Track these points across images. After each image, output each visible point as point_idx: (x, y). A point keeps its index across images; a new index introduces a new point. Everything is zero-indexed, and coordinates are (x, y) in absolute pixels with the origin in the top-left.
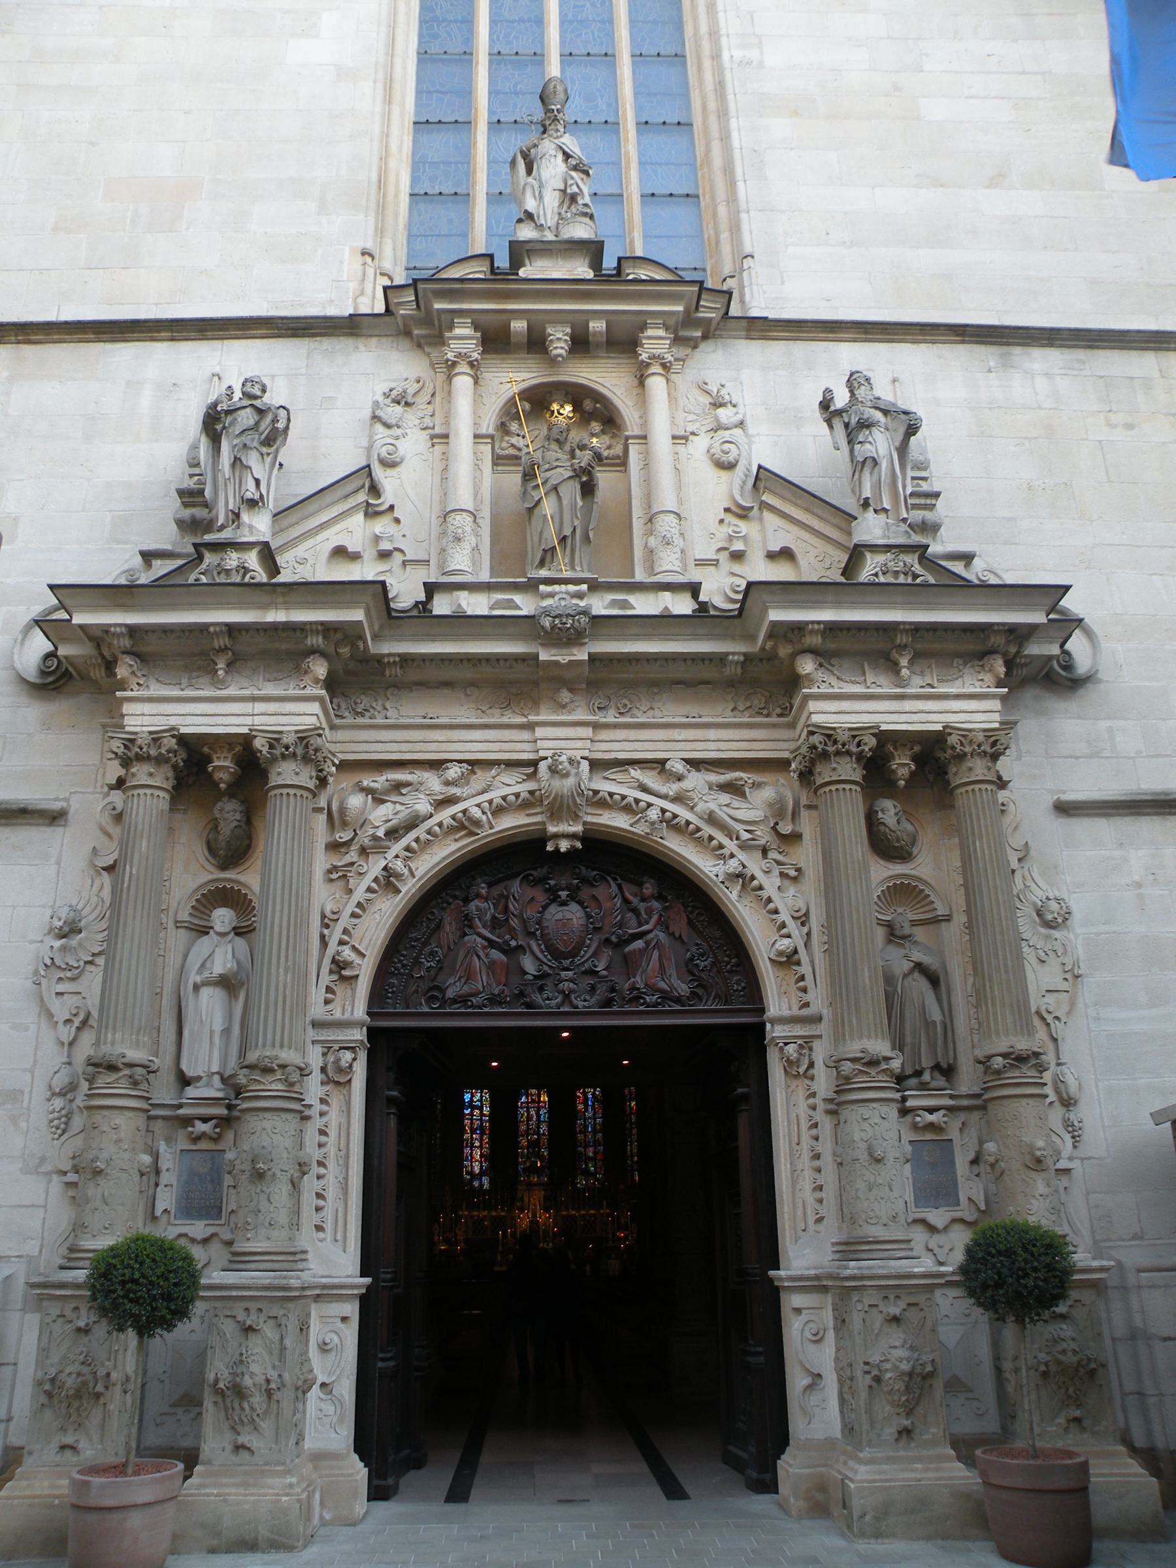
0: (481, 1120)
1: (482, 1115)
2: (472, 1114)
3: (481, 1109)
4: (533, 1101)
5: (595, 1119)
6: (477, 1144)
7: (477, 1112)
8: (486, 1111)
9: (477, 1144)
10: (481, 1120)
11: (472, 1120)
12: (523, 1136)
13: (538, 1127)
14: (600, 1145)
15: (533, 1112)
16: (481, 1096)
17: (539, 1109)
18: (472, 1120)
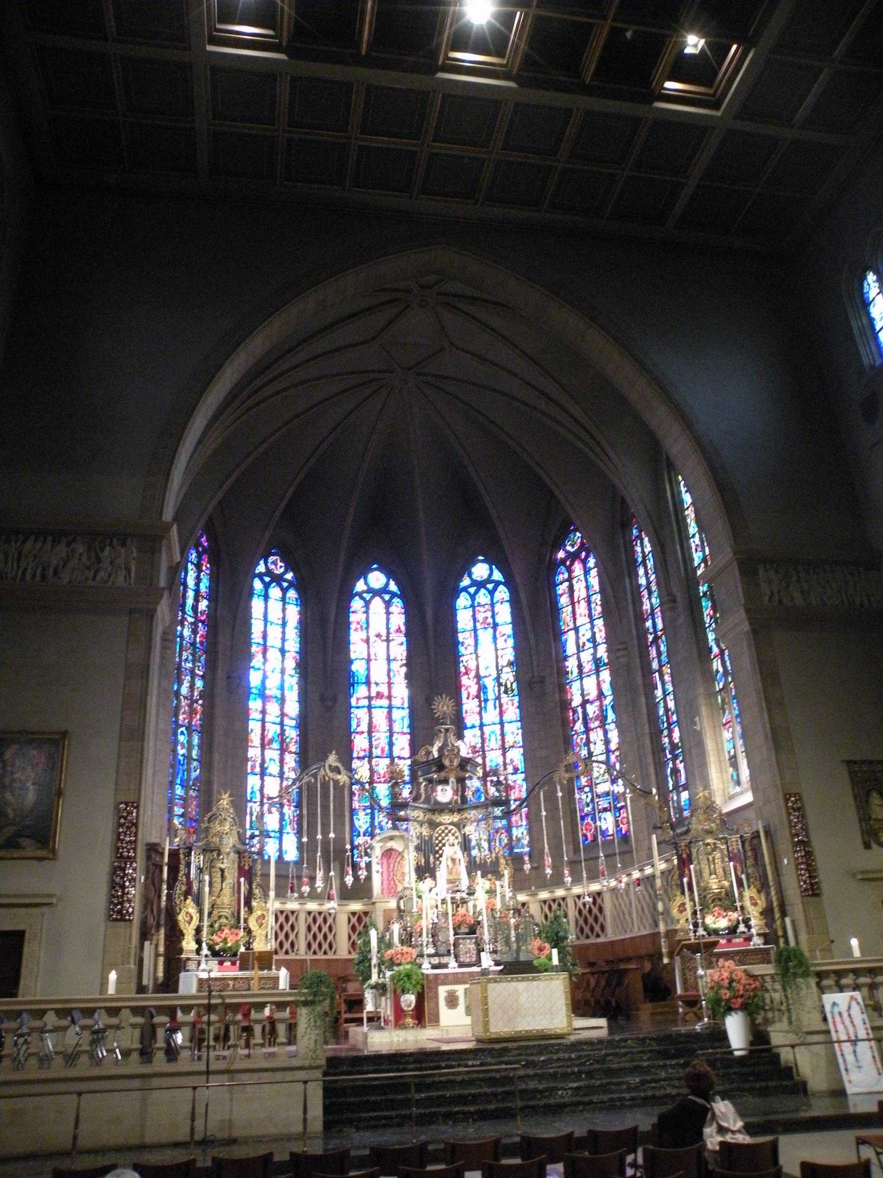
0: (282, 724)
1: (283, 715)
2: (263, 712)
3: (282, 700)
4: (379, 695)
5: (502, 723)
6: (273, 768)
7: (273, 709)
8: (293, 708)
9: (273, 768)
10: (282, 724)
11: (263, 721)
12: (358, 758)
13: (391, 744)
14: (516, 770)
15: (380, 716)
16: (283, 681)
17: (390, 707)
18: (263, 721)
